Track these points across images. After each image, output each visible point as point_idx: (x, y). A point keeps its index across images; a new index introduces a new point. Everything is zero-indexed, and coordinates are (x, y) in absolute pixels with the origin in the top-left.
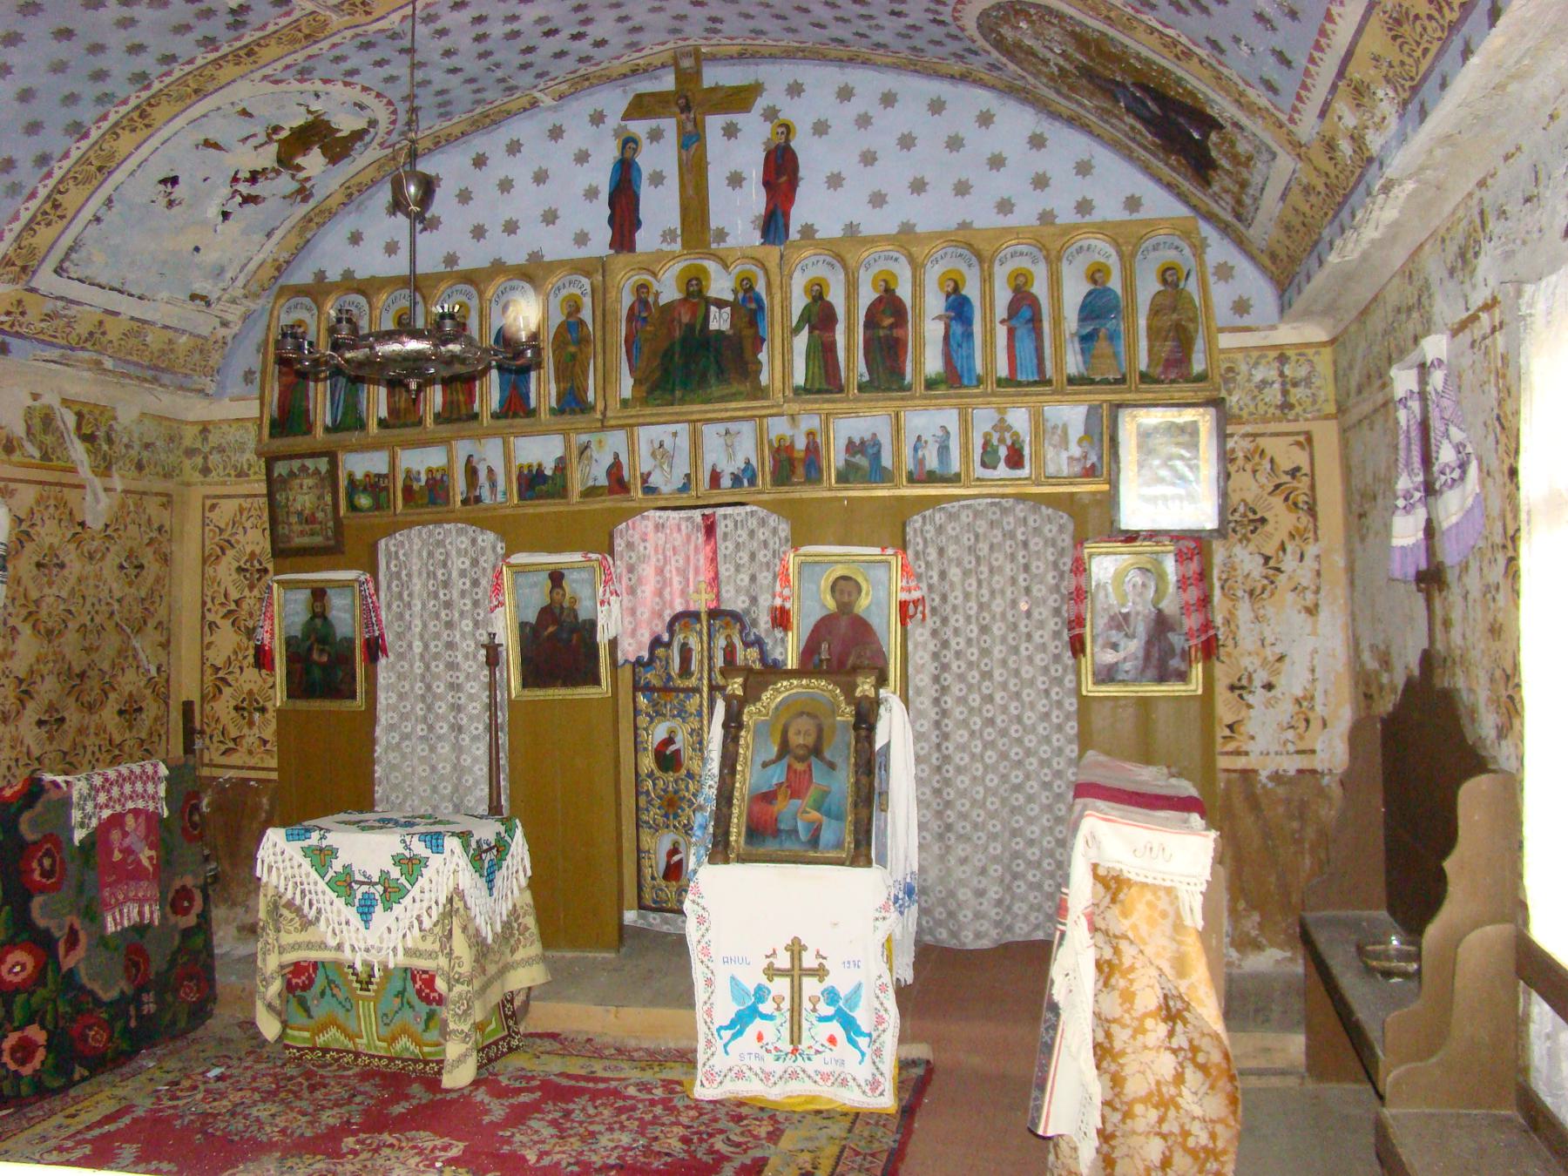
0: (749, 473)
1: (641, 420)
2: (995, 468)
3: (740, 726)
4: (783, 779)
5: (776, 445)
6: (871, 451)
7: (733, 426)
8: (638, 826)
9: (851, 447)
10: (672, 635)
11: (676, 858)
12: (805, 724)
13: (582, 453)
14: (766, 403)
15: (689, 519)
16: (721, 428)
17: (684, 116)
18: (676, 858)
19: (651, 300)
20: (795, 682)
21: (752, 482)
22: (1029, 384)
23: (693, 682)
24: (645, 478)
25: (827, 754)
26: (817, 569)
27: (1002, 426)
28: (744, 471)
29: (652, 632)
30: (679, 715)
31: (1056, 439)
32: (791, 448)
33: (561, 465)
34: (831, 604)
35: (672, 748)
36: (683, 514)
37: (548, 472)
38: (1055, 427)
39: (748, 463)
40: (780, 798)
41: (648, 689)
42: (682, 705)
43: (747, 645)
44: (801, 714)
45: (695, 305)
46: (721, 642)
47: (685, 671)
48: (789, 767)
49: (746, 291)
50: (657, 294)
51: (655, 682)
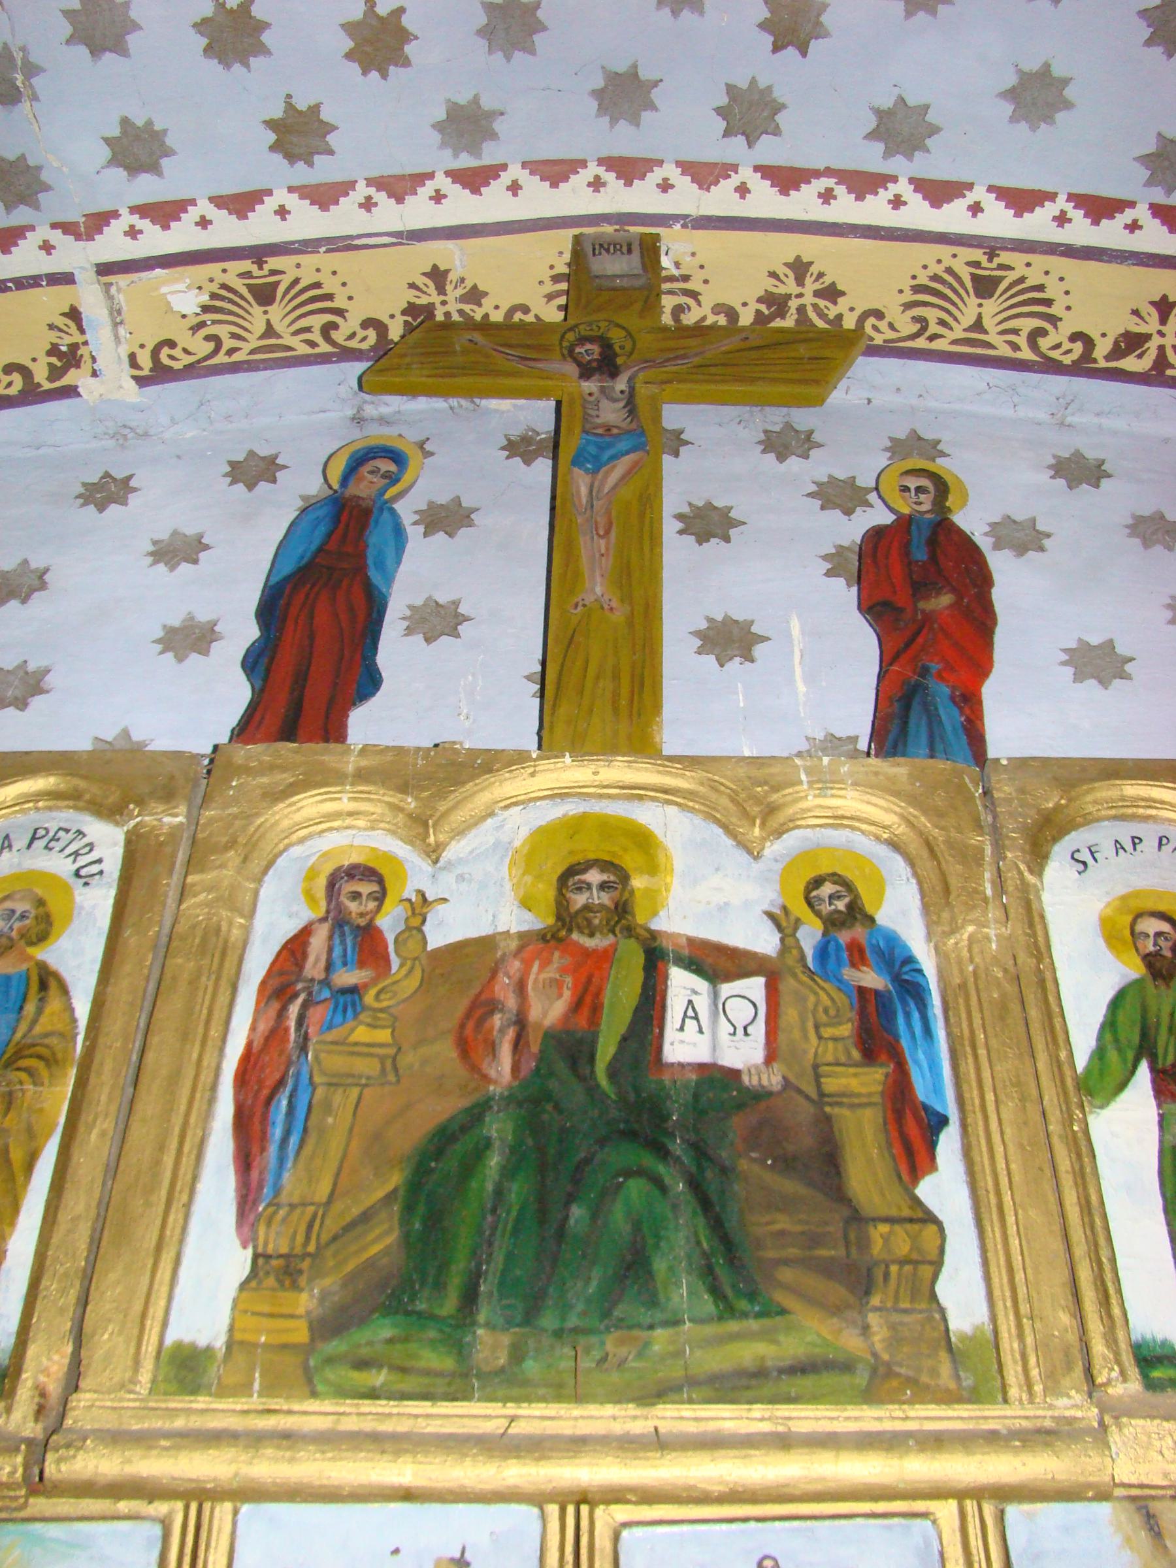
14: (992, 1416)
17: (590, 386)
19: (389, 922)
45: (606, 957)
49: (832, 923)
50: (421, 906)
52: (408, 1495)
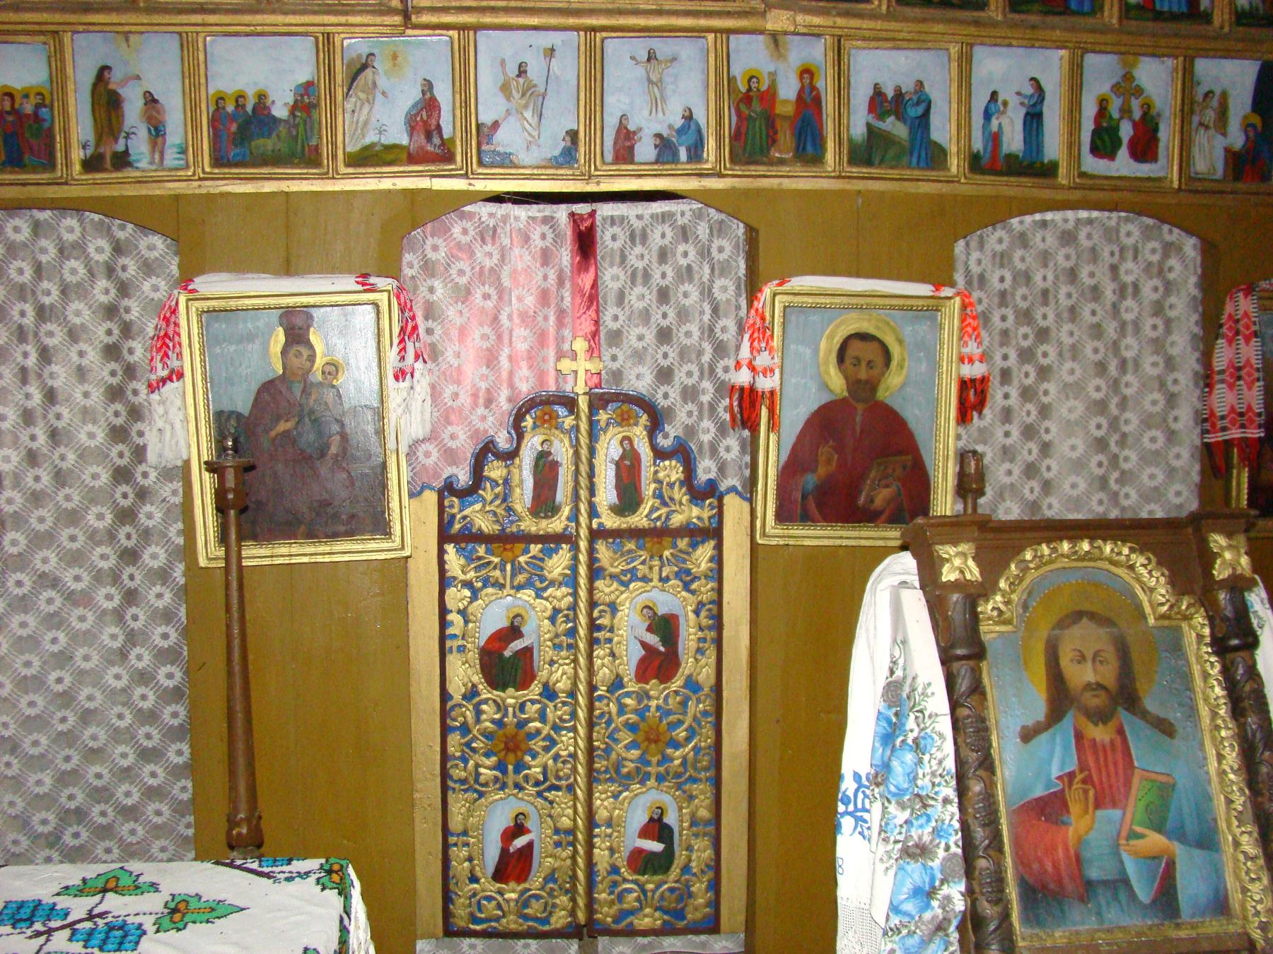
0: (691, 138)
1: (488, 19)
2: (1112, 157)
3: (978, 652)
4: (1072, 766)
5: (743, 88)
6: (917, 111)
7: (664, 47)
8: (445, 789)
9: (878, 102)
10: (519, 432)
11: (520, 842)
12: (1079, 638)
13: (354, 78)
15: (546, 220)
16: (640, 47)
18: (520, 842)
20: (1066, 546)
21: (696, 153)
22: (1174, 17)
23: (556, 525)
24: (485, 133)
25: (1151, 704)
26: (815, 318)
27: (1127, 86)
28: (680, 132)
29: (475, 434)
30: (528, 584)
31: (1210, 116)
32: (769, 96)
33: (306, 101)
34: (837, 383)
35: (517, 645)
36: (535, 210)
37: (280, 111)
38: (1208, 94)
39: (689, 117)
40: (1075, 808)
41: (468, 537)
42: (537, 564)
43: (660, 454)
44: (1078, 615)
46: (609, 448)
47: (544, 503)
48: (1079, 736)
51: (484, 524)
52: (535, 28)
